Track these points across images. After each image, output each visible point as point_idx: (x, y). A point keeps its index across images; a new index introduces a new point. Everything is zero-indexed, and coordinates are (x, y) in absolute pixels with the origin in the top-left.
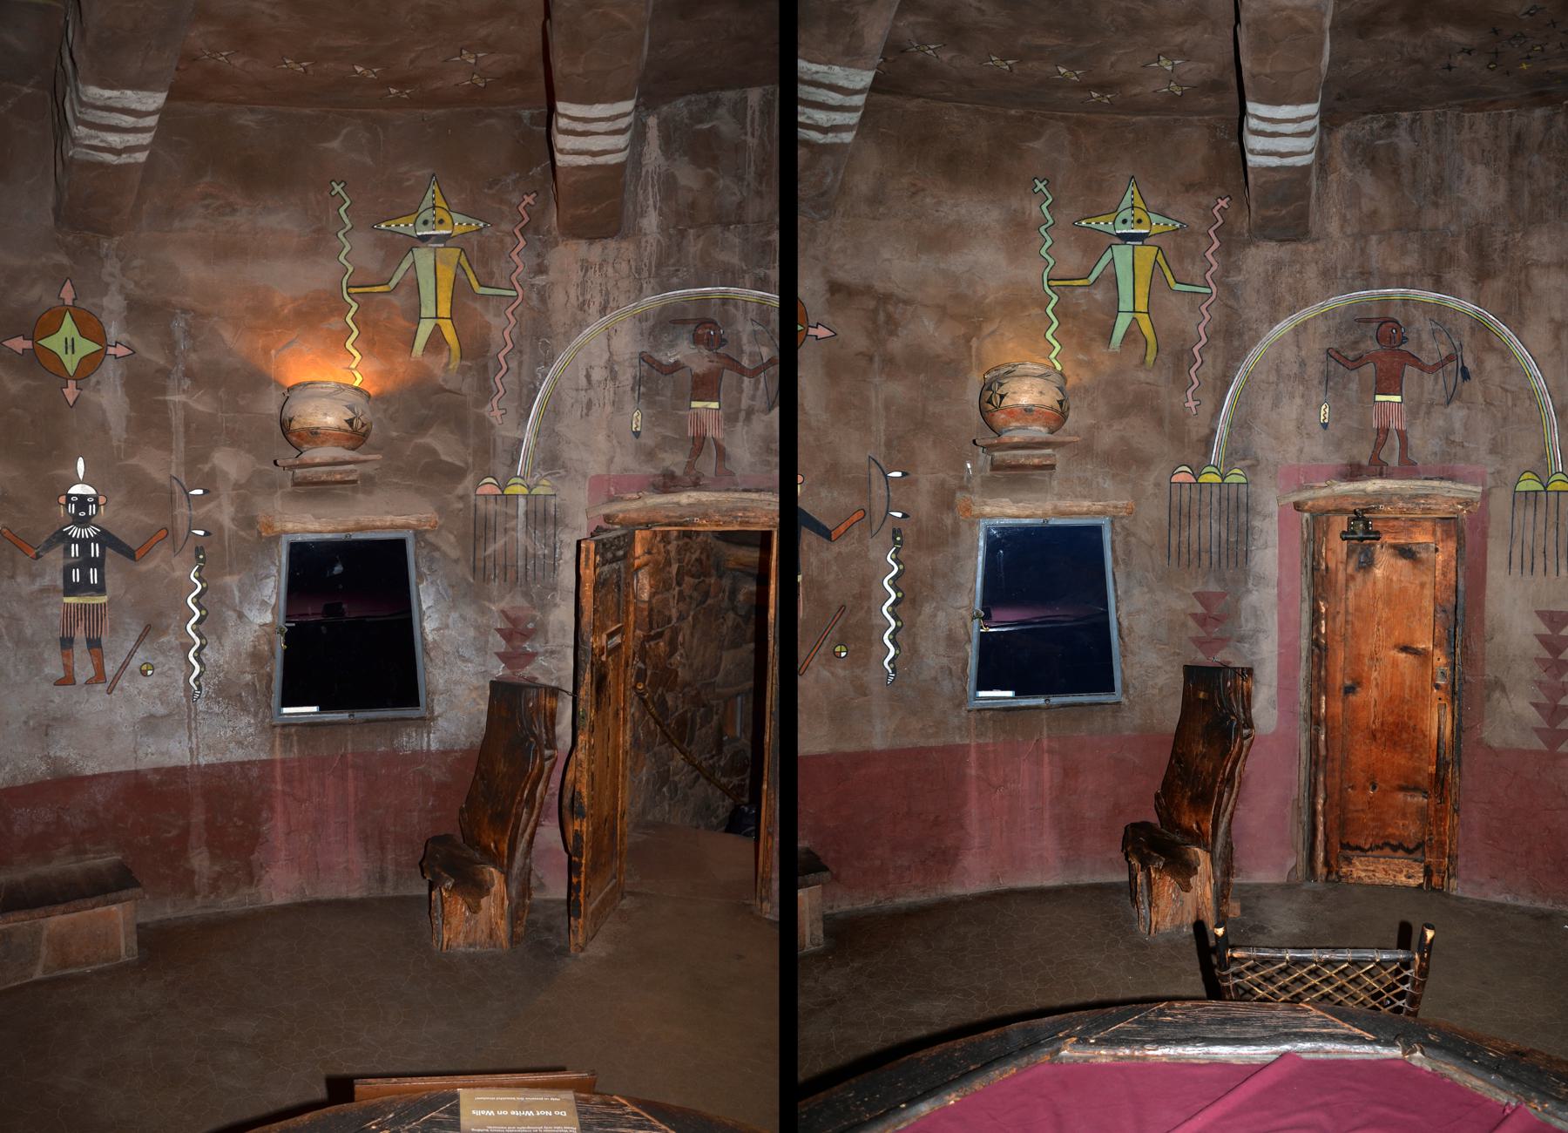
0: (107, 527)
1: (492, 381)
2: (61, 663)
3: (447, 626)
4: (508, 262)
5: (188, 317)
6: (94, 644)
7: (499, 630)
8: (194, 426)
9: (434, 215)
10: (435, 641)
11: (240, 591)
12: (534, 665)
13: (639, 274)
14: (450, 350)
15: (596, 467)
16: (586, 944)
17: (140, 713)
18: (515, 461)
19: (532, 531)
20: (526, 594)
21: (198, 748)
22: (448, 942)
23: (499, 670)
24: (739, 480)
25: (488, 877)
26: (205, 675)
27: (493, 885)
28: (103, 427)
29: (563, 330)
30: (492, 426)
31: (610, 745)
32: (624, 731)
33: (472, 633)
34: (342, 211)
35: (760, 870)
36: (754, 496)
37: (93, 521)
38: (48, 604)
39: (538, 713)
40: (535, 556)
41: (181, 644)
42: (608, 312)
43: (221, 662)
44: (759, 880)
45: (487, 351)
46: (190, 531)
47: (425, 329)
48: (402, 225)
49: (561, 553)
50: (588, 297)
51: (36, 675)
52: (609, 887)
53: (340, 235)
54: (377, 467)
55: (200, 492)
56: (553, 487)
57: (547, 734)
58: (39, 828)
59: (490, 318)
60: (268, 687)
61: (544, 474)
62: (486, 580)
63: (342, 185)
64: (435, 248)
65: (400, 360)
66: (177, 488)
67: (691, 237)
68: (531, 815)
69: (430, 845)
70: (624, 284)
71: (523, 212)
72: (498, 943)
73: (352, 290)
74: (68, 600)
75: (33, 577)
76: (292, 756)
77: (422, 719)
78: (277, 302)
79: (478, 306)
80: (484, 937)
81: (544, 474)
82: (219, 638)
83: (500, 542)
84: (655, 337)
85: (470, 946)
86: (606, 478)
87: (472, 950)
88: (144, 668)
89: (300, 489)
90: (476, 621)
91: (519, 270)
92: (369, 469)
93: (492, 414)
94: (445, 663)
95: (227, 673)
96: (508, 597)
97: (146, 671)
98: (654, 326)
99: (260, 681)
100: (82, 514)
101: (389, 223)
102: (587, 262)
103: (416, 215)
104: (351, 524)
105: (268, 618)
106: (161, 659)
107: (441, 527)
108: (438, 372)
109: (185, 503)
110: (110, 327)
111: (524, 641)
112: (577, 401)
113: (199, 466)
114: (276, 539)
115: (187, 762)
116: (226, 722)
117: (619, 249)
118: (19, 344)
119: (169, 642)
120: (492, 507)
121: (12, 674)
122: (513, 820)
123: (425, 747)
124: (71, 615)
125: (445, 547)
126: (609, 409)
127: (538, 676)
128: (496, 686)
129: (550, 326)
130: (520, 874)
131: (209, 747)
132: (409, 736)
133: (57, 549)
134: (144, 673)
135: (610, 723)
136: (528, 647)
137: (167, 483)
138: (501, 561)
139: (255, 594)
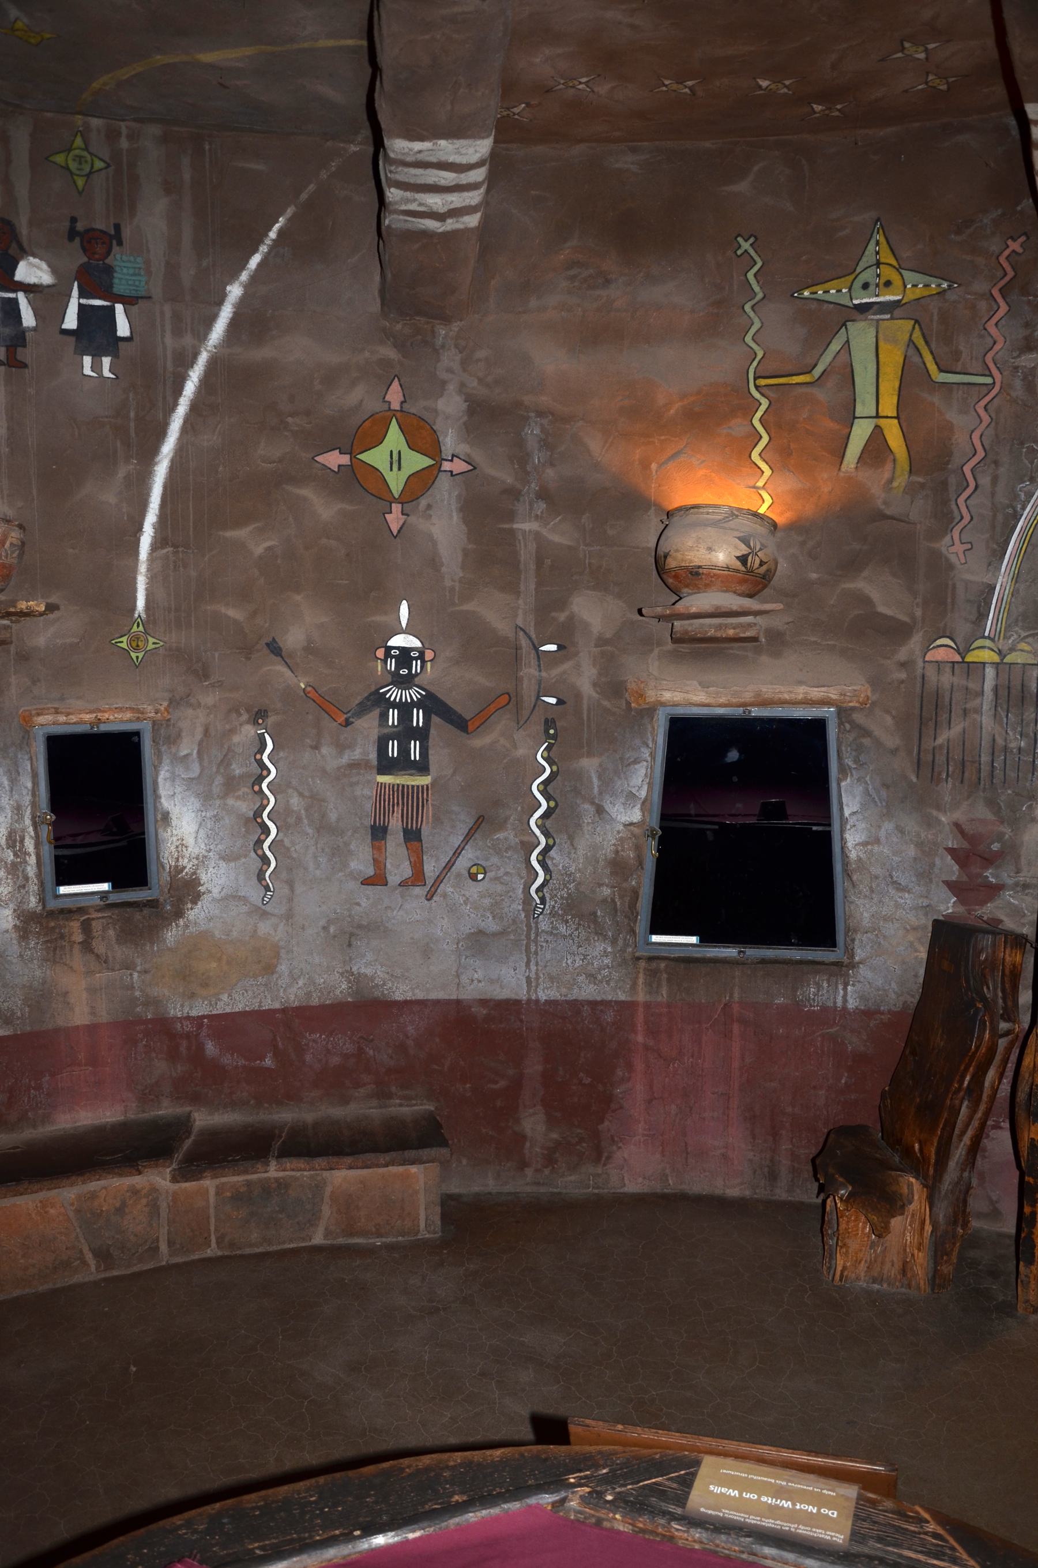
0: (432, 689)
1: (953, 503)
2: (370, 858)
3: (877, 841)
4: (981, 336)
5: (545, 421)
6: (412, 836)
7: (951, 851)
8: (548, 562)
9: (878, 276)
10: (860, 859)
11: (600, 778)
12: (998, 902)
14: (894, 460)
17: (466, 929)
18: (983, 616)
19: (1003, 715)
20: (992, 803)
21: (538, 978)
23: (948, 906)
26: (550, 885)
28: (434, 562)
30: (951, 567)
33: (911, 851)
34: (750, 276)
37: (417, 680)
38: (357, 783)
40: (1005, 749)
41: (522, 843)
43: (573, 869)
45: (948, 463)
46: (538, 698)
47: (861, 433)
48: (833, 291)
51: (341, 870)
53: (748, 308)
54: (790, 620)
55: (553, 647)
58: (335, 1060)
59: (953, 416)
60: (633, 906)
61: (1023, 634)
62: (934, 778)
63: (752, 240)
64: (878, 321)
65: (825, 476)
66: (524, 642)
69: (832, 1136)
71: (1006, 265)
73: (762, 382)
74: (382, 779)
75: (341, 747)
76: (659, 999)
77: (838, 964)
78: (661, 400)
79: (936, 399)
81: (1023, 634)
82: (571, 838)
83: (957, 729)
88: (474, 870)
89: (685, 648)
90: (918, 835)
91: (997, 347)
92: (778, 623)
93: (952, 549)
94: (872, 891)
95: (579, 884)
97: (476, 875)
99: (621, 897)
100: (404, 672)
101: (814, 289)
103: (853, 276)
104: (748, 696)
105: (635, 815)
106: (495, 860)
107: (874, 704)
108: (876, 491)
109: (534, 662)
110: (446, 436)
111: (986, 868)
113: (553, 614)
114: (650, 711)
115: (522, 994)
116: (575, 948)
118: (334, 460)
119: (506, 839)
120: (947, 679)
121: (311, 866)
123: (839, 1003)
124: (386, 798)
125: (877, 732)
131: (552, 979)
132: (819, 987)
133: (372, 714)
134: (473, 877)
136: (990, 875)
137: (511, 635)
139: (619, 783)
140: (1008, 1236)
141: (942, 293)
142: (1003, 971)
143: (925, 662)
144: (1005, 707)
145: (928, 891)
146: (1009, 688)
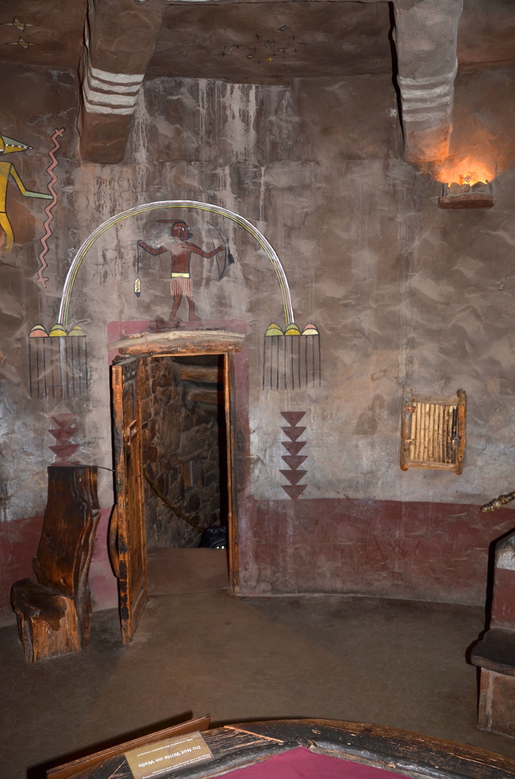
3: (13, 432)
4: (45, 175)
7: (51, 431)
12: (77, 453)
13: (136, 189)
14: (6, 235)
15: (112, 317)
16: (132, 636)
18: (56, 314)
19: (70, 361)
20: (69, 405)
22: (37, 655)
23: (53, 459)
24: (204, 323)
25: (62, 604)
27: (66, 609)
29: (86, 224)
30: (39, 290)
31: (135, 501)
32: (141, 490)
33: (32, 435)
35: (231, 566)
36: (215, 333)
39: (85, 486)
40: (73, 378)
42: (116, 212)
44: (231, 574)
45: (33, 237)
49: (91, 376)
50: (102, 202)
52: (141, 595)
56: (84, 331)
57: (93, 498)
59: (34, 213)
61: (77, 322)
67: (168, 167)
68: (86, 556)
70: (126, 195)
71: (55, 141)
72: (73, 648)
79: (25, 204)
80: (63, 646)
81: (77, 322)
83: (48, 371)
84: (147, 231)
85: (54, 654)
86: (119, 323)
87: (55, 657)
90: (34, 426)
91: (54, 181)
93: (38, 281)
94: (14, 458)
96: (56, 408)
98: (146, 224)
102: (101, 179)
107: (5, 361)
111: (70, 437)
112: (97, 272)
117: (121, 172)
120: (41, 346)
122: (75, 561)
125: (8, 375)
126: (119, 277)
127: (80, 460)
128: (53, 470)
129: (77, 221)
130: (84, 598)
135: (134, 486)
136: (72, 441)
138: (50, 383)
140: (110, 611)
141: (24, 151)
142: (91, 485)
143: (30, 338)
144: (71, 357)
145: (42, 453)
146: (72, 348)
